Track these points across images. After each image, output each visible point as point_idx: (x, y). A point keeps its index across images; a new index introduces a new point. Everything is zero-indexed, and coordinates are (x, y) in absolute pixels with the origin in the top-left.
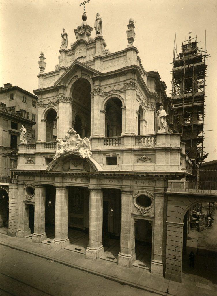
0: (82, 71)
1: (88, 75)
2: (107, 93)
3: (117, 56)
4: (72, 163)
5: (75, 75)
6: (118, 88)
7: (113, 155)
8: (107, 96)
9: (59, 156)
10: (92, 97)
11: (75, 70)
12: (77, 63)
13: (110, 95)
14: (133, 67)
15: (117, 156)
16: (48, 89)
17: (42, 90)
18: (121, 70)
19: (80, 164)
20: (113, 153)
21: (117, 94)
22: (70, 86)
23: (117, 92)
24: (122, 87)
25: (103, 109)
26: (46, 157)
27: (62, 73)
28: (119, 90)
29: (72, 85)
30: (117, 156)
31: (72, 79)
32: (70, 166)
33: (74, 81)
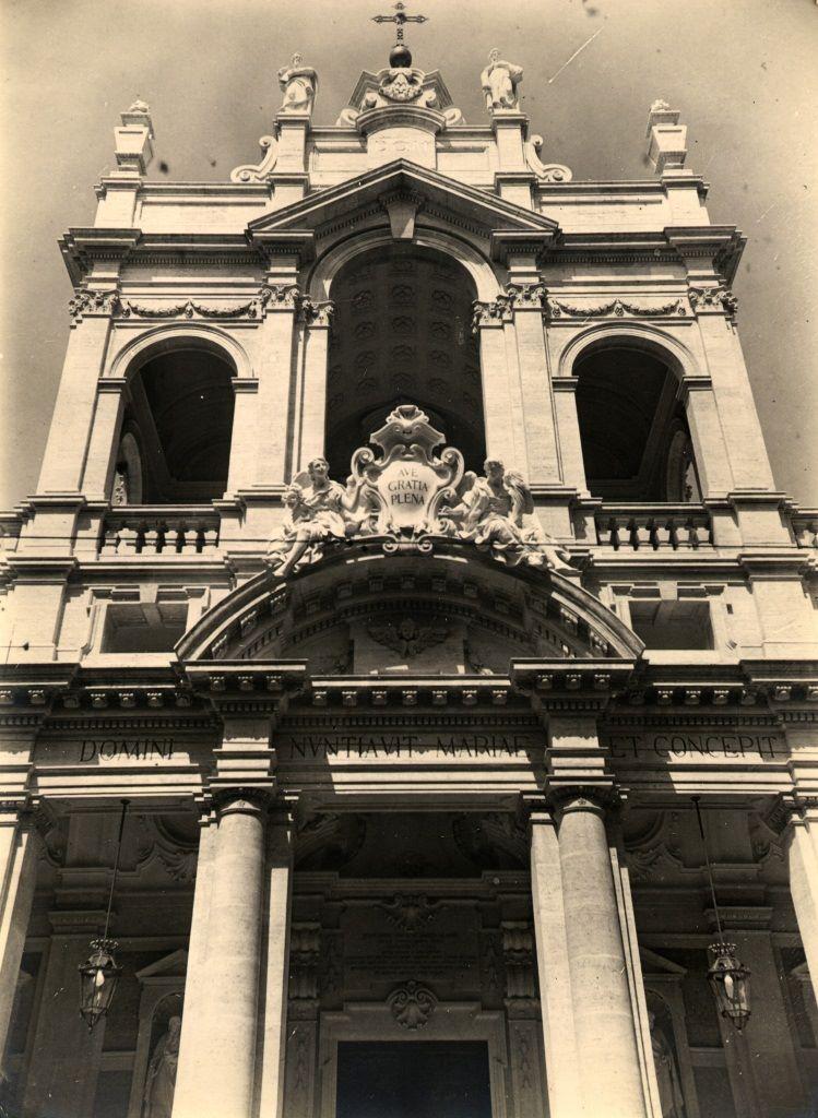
0: (417, 213)
1: (450, 234)
2: (583, 313)
3: (615, 198)
4: (371, 635)
5: (379, 220)
6: (642, 303)
7: (681, 593)
8: (582, 330)
9: (317, 557)
10: (482, 323)
11: (378, 201)
12: (404, 172)
13: (600, 323)
14: (728, 234)
15: (711, 599)
16: (193, 241)
17: (142, 238)
18: (665, 234)
19: (447, 636)
20: (679, 584)
21: (646, 323)
22: (336, 262)
23: (644, 320)
24: (674, 304)
25: (568, 372)
26: (116, 597)
27: (286, 197)
28: (655, 313)
29: (347, 259)
30: (716, 603)
31: (354, 235)
32: (351, 654)
33: (363, 246)
